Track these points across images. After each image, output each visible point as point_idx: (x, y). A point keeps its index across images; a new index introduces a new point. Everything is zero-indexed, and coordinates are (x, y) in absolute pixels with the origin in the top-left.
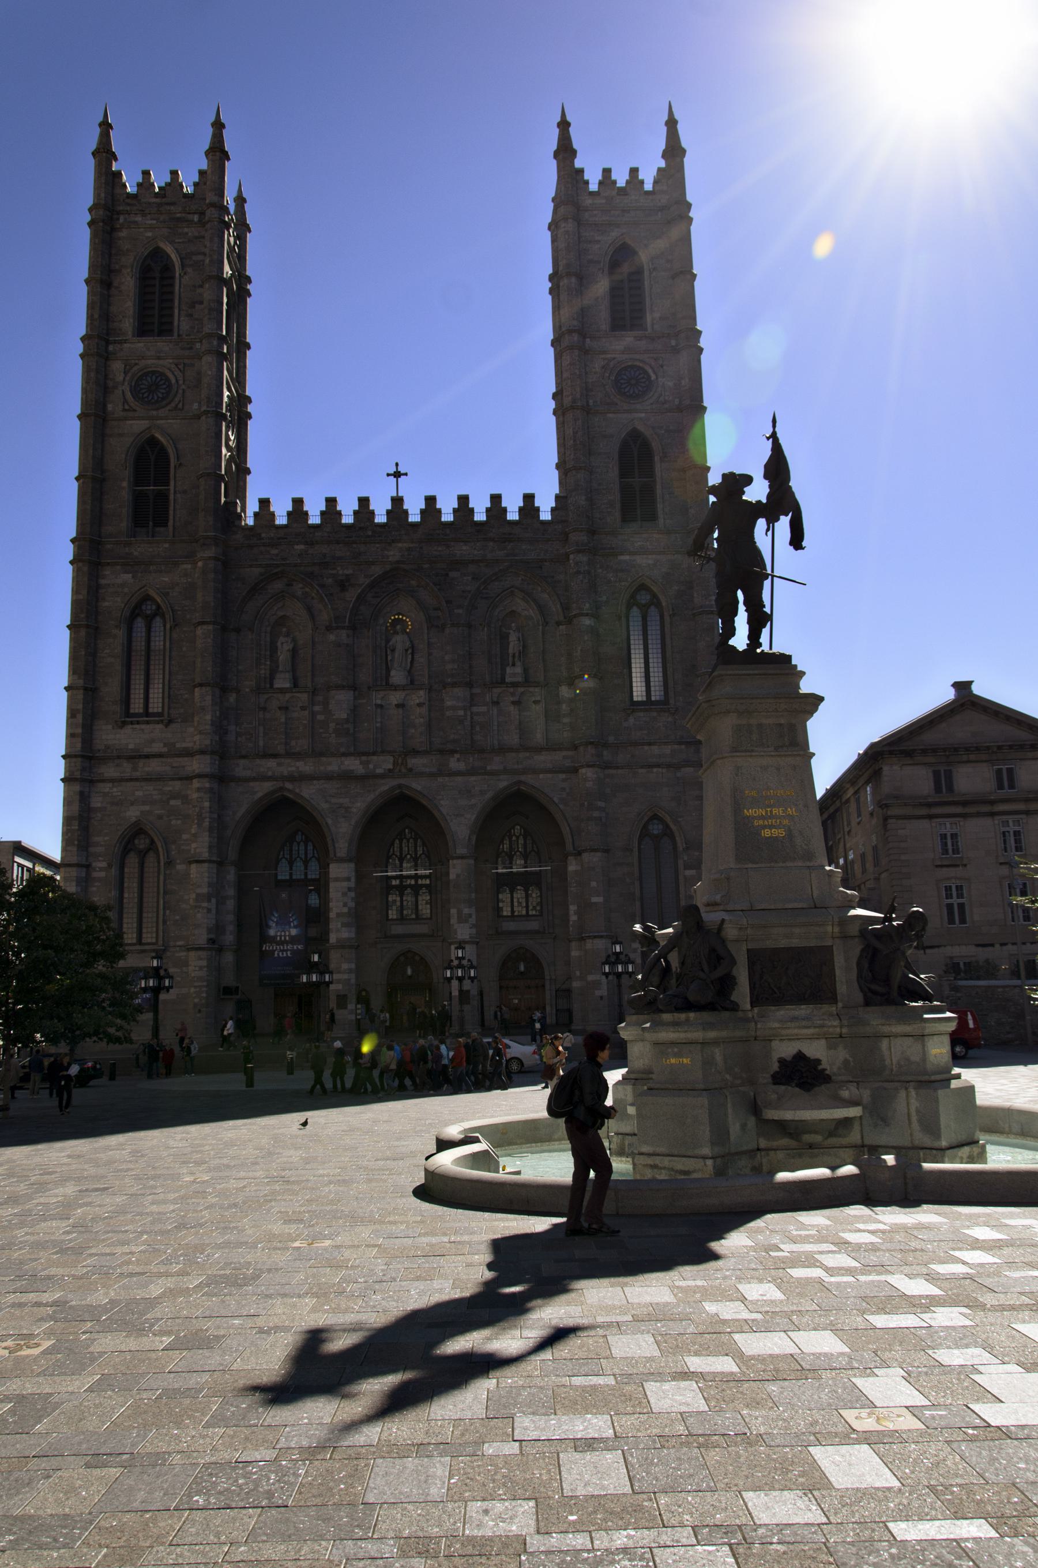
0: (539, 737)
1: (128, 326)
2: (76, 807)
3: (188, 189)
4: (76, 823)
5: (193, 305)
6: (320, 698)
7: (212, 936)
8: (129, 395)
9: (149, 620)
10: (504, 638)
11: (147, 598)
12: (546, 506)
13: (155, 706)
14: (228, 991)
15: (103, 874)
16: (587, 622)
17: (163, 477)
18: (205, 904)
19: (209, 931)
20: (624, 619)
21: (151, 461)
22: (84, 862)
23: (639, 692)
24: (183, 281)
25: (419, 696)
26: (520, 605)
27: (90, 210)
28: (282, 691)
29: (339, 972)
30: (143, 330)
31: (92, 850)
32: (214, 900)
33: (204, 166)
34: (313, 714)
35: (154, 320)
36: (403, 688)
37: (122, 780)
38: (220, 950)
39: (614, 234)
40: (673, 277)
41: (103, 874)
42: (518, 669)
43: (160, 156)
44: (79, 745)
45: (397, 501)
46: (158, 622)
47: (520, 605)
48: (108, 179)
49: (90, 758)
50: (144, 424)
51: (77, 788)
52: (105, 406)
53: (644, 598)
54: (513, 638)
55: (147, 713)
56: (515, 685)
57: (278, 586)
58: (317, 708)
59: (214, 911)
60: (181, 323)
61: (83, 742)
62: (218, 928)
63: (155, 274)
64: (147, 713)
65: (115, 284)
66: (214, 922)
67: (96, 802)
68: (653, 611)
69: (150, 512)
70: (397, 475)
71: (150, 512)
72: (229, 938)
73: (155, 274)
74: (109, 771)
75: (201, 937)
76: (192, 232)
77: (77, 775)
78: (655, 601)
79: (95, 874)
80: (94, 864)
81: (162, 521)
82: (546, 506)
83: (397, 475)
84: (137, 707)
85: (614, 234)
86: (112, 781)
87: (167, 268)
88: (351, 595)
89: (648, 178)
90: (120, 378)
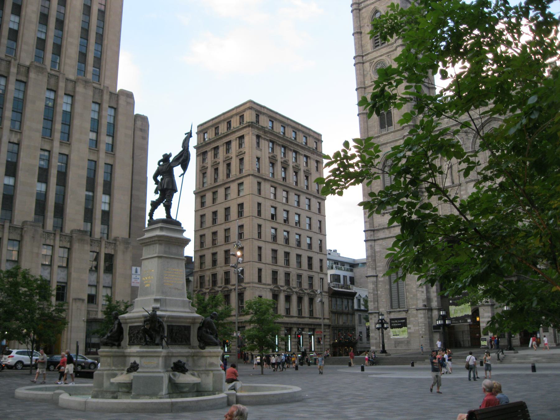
2: (369, 252)
4: (370, 258)
6: (463, 188)
7: (425, 303)
8: (372, 75)
14: (437, 327)
15: (382, 279)
18: (420, 289)
19: (424, 301)
22: (375, 274)
27: (352, 5)
29: (483, 318)
31: (377, 269)
32: (424, 287)
37: (385, 238)
38: (431, 310)
41: (382, 279)
44: (368, 226)
49: (374, 231)
51: (370, 243)
52: (364, 82)
58: (462, 193)
59: (425, 292)
61: (370, 224)
62: (429, 299)
65: (363, 32)
66: (426, 297)
67: (377, 248)
72: (435, 304)
75: (421, 305)
77: (369, 239)
79: (381, 279)
80: (379, 275)
86: (382, 239)
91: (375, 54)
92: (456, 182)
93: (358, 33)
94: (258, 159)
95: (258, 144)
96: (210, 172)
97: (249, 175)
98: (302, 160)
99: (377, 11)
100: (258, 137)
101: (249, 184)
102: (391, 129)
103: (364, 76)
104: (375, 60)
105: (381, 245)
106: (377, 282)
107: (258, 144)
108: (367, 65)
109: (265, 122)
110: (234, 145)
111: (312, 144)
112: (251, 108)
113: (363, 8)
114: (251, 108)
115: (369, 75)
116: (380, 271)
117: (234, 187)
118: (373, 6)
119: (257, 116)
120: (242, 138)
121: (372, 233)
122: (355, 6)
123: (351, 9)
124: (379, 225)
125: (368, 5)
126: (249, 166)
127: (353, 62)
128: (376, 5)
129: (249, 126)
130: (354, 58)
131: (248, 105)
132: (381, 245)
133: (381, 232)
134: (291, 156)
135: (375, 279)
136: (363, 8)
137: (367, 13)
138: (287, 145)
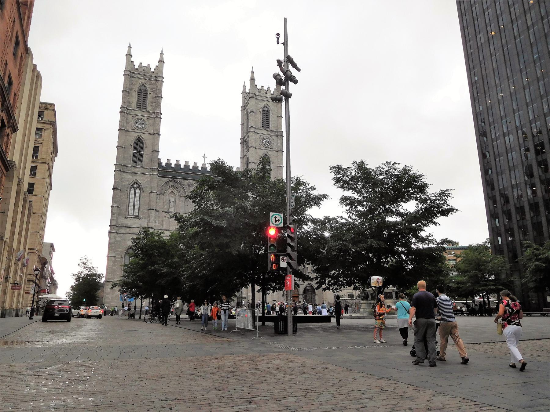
1: (134, 105)
3: (153, 70)
5: (152, 102)
9: (135, 189)
13: (136, 213)
17: (142, 149)
21: (139, 144)
24: (150, 95)
27: (124, 71)
30: (138, 107)
33: (157, 64)
35: (142, 104)
39: (264, 103)
43: (145, 58)
45: (204, 164)
46: (138, 190)
48: (130, 63)
50: (137, 134)
55: (133, 215)
57: (171, 183)
60: (149, 108)
63: (142, 93)
64: (133, 215)
69: (138, 158)
70: (204, 157)
71: (138, 158)
73: (142, 93)
74: (123, 230)
76: (153, 82)
81: (141, 161)
84: (131, 213)
85: (264, 103)
89: (272, 90)
90: (131, 119)
91: (138, 113)
93: (126, 92)
97: (46, 163)
99: (143, 85)
102: (139, 165)
103: (127, 123)
104: (138, 117)
105: (121, 237)
106: (115, 261)
108: (130, 117)
113: (133, 77)
115: (130, 124)
116: (118, 254)
118: (141, 81)
121: (116, 228)
122: (128, 73)
124: (122, 224)
125: (138, 78)
127: (120, 110)
128: (144, 81)
129: (51, 124)
130: (121, 108)
132: (121, 237)
133: (123, 229)
135: (113, 259)
136: (133, 77)
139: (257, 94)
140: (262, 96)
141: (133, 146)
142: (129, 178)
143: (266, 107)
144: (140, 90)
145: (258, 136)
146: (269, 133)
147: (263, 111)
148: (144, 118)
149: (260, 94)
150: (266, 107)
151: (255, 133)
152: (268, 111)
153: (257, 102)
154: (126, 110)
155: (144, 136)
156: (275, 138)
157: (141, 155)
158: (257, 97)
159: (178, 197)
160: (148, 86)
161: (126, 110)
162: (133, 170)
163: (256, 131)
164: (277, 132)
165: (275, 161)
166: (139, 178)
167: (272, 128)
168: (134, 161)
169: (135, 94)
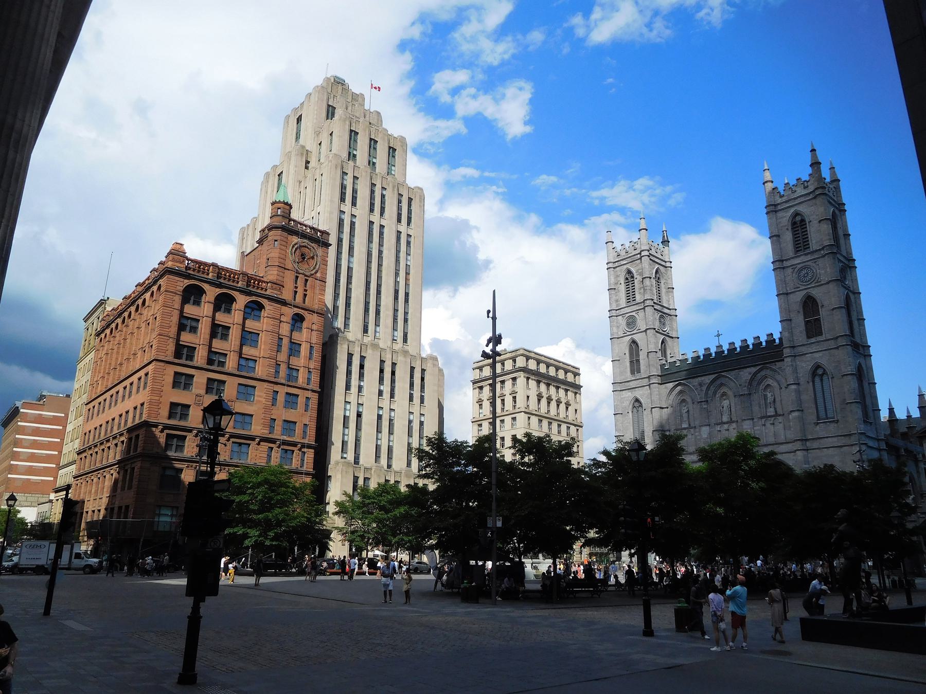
0: (782, 439)
1: (623, 303)
10: (765, 397)
11: (637, 400)
12: (776, 336)
16: (793, 387)
17: (638, 355)
20: (811, 384)
23: (822, 414)
25: (734, 425)
26: (770, 382)
28: (685, 429)
34: (696, 437)
36: (727, 423)
39: (792, 210)
40: (820, 222)
42: (772, 409)
47: (770, 382)
53: (820, 372)
54: (769, 395)
56: (770, 416)
57: (679, 388)
68: (825, 377)
78: (825, 373)
81: (639, 372)
82: (776, 336)
83: (718, 335)
85: (792, 210)
87: (633, 277)
88: (704, 388)
92: (692, 425)
94: (528, 397)
95: (528, 383)
96: (487, 405)
98: (562, 392)
99: (629, 272)
100: (528, 379)
101: (521, 417)
107: (528, 383)
109: (532, 365)
110: (509, 384)
111: (570, 377)
112: (522, 355)
114: (522, 355)
117: (508, 420)
118: (625, 267)
119: (527, 360)
120: (514, 379)
123: (606, 267)
126: (521, 403)
128: (628, 266)
131: (522, 352)
134: (553, 390)
137: (622, 272)
138: (550, 381)
139: (779, 200)
140: (786, 202)
141: (628, 354)
142: (629, 395)
143: (797, 214)
144: (627, 279)
145: (789, 271)
146: (809, 257)
147: (794, 224)
148: (633, 314)
149: (784, 199)
150: (797, 214)
151: (784, 268)
152: (803, 220)
153: (780, 214)
154: (614, 313)
155: (637, 337)
156: (820, 262)
157: (638, 361)
158: (779, 207)
159: (690, 406)
160: (633, 270)
161: (614, 313)
162: (632, 384)
163: (786, 264)
164: (823, 248)
165: (825, 303)
166: (638, 394)
167: (814, 245)
168: (632, 372)
169: (622, 288)
